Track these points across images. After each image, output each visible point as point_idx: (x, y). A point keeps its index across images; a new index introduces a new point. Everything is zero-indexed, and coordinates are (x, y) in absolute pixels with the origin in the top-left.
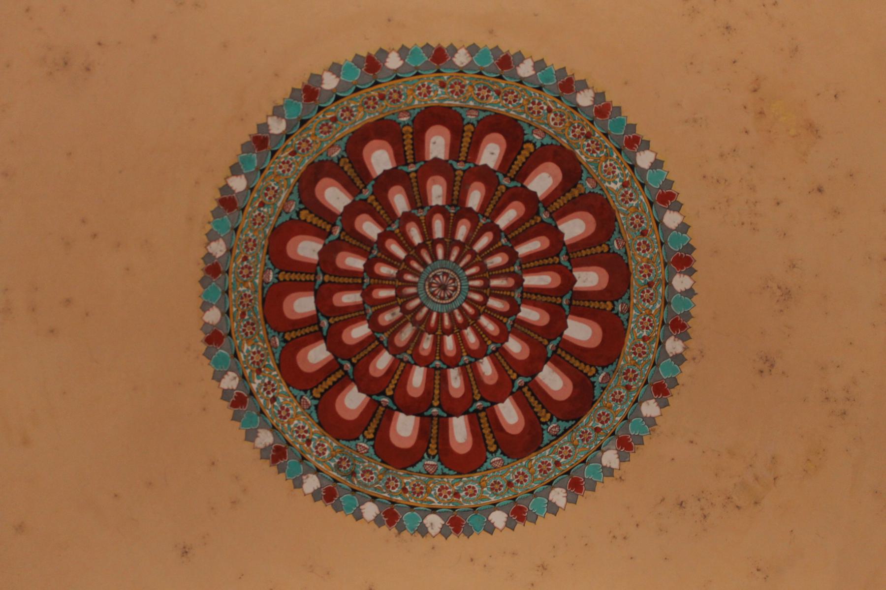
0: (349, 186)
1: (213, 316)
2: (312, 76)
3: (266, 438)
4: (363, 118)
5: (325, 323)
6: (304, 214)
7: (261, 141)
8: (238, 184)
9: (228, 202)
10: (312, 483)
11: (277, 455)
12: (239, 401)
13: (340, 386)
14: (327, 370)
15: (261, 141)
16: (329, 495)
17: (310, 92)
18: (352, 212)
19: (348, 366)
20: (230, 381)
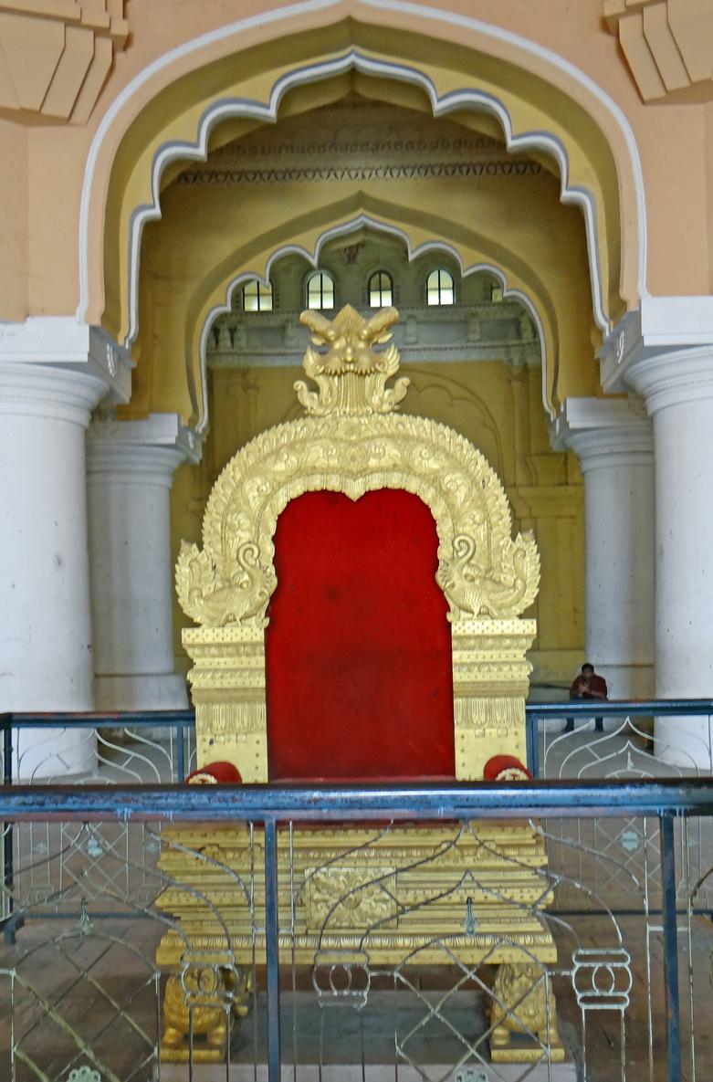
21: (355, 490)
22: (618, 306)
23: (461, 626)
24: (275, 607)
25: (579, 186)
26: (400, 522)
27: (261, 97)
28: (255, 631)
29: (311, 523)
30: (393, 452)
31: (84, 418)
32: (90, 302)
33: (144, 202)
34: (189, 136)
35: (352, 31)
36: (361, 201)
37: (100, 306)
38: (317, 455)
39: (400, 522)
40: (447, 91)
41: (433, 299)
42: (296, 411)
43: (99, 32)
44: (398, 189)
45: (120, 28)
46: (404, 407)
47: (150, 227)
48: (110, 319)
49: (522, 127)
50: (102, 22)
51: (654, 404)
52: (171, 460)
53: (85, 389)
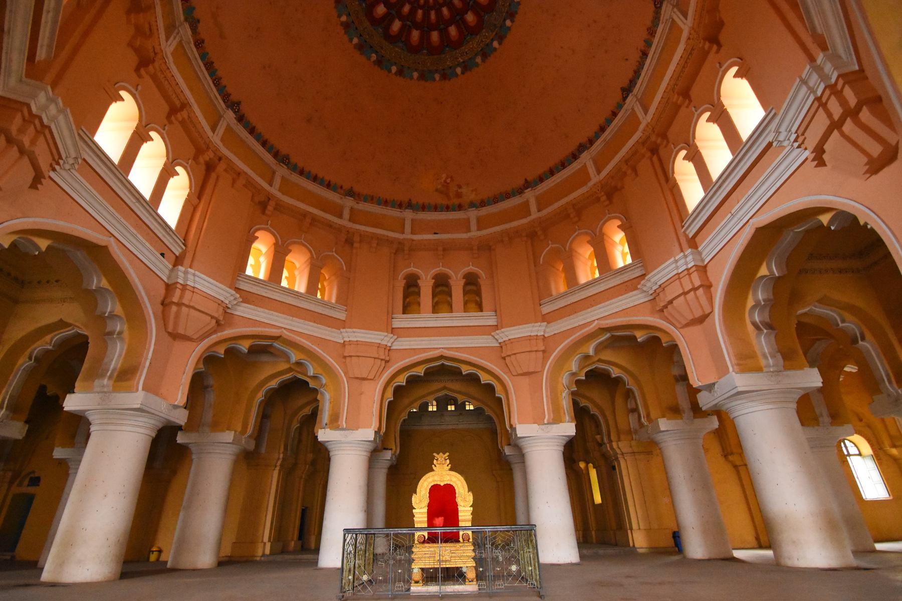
0: (391, 22)
1: (437, 76)
2: (355, 48)
3: (479, 60)
4: (367, 24)
5: (442, 26)
6: (403, 39)
7: (379, 63)
8: (394, 69)
9: (400, 73)
10: (496, 44)
11: (485, 56)
12: (466, 68)
13: (464, 22)
14: (458, 28)
15: (379, 63)
16: (501, 39)
17: (360, 47)
18: (401, 17)
19: (458, 18)
20: (459, 70)
21: (442, 484)
22: (511, 426)
23: (460, 508)
24: (429, 506)
25: (499, 393)
26: (449, 490)
27: (420, 371)
28: (425, 510)
29: (435, 490)
30: (448, 478)
31: (369, 454)
32: (375, 425)
33: (390, 396)
34: (402, 380)
35: (442, 357)
36: (445, 388)
37: (378, 425)
38: (436, 478)
39: (449, 490)
40: (465, 370)
41: (467, 408)
42: (433, 470)
43: (382, 360)
44: (456, 386)
45: (387, 359)
46: (451, 470)
47: (390, 402)
48: (380, 428)
49: (485, 378)
50: (383, 357)
51: (525, 451)
52: (387, 464)
53: (370, 447)
